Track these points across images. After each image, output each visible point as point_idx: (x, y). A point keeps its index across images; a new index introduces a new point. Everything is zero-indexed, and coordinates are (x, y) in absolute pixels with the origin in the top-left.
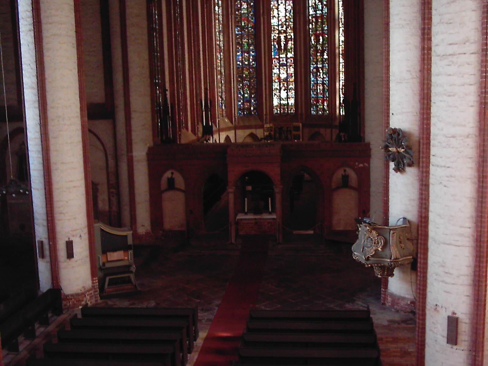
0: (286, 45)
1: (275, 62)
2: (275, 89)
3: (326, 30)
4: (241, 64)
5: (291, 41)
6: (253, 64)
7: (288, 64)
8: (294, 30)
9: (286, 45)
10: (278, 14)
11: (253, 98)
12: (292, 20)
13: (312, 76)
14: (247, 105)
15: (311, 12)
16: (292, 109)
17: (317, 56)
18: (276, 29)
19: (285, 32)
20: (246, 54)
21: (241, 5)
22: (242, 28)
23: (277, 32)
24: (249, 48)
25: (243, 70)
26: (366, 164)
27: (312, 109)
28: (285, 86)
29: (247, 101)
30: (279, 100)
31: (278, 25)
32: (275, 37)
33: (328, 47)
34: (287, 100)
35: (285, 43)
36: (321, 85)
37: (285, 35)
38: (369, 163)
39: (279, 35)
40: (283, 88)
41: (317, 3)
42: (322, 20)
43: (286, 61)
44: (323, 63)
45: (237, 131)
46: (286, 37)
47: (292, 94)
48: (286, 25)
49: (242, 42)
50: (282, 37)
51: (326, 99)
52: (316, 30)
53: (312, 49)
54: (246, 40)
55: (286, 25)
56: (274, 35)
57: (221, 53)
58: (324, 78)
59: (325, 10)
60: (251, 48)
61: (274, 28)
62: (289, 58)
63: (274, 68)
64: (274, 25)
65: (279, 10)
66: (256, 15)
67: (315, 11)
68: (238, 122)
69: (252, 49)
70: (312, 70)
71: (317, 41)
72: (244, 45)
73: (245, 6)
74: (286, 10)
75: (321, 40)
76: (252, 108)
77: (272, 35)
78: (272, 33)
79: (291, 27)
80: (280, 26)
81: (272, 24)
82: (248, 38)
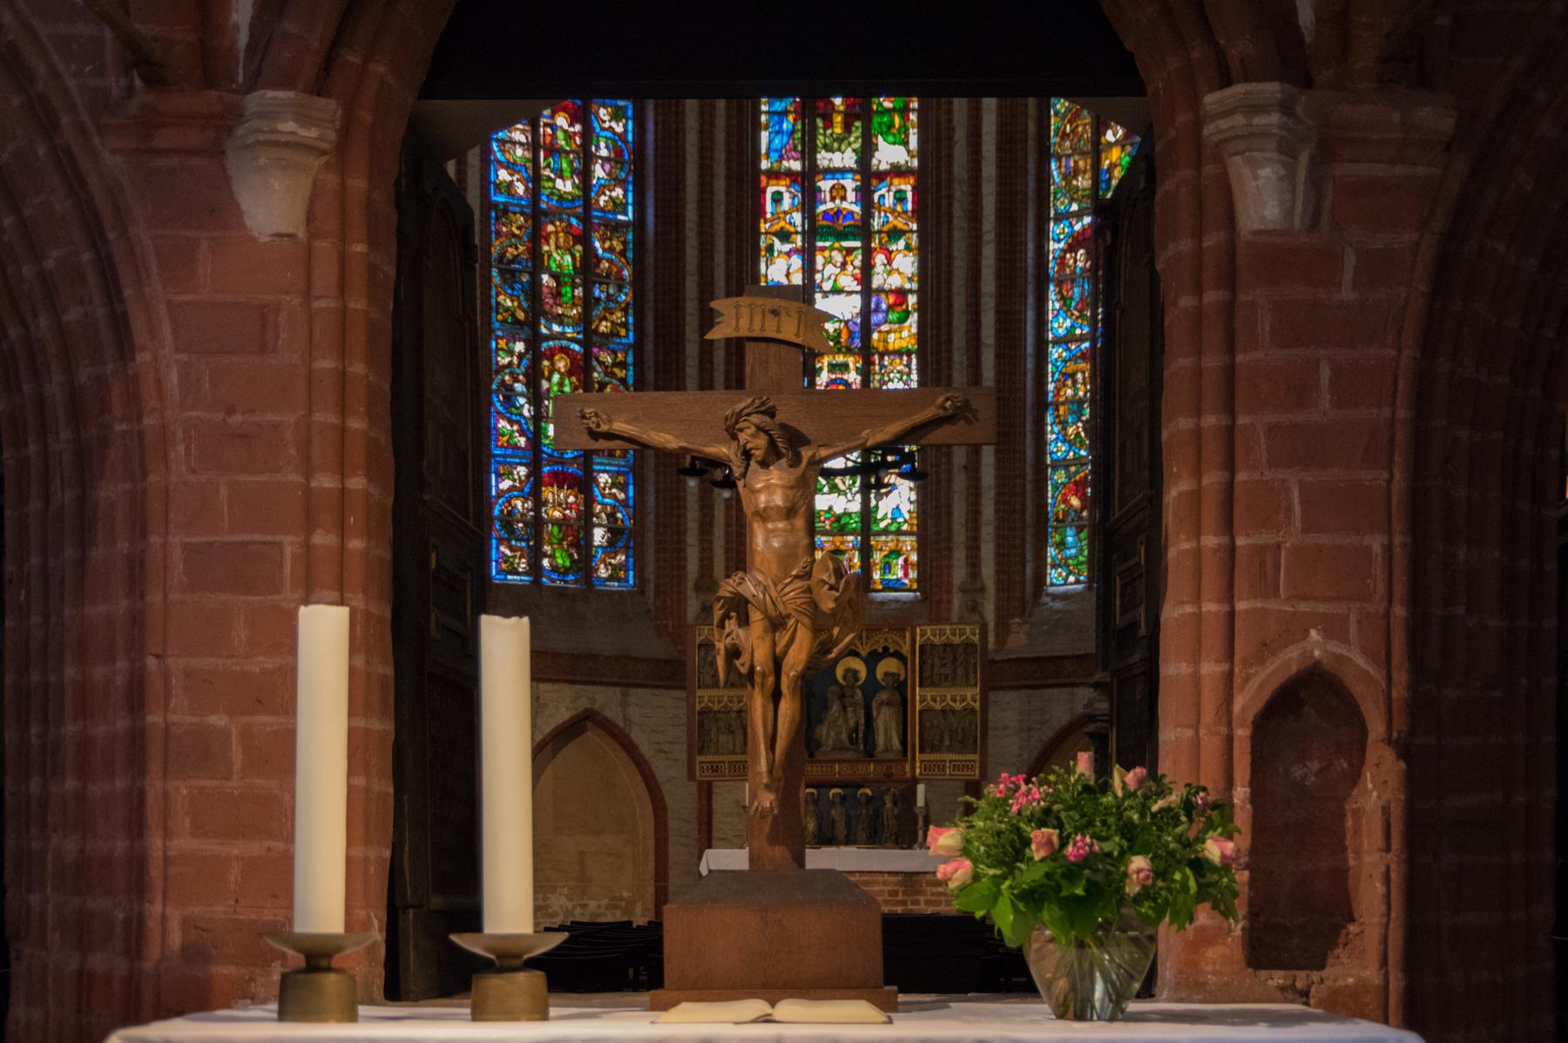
1: (781, 204)
4: (520, 189)
6: (619, 206)
7: (876, 223)
13: (1053, 303)
16: (897, 553)
20: (561, 121)
27: (1051, 551)
29: (560, 480)
43: (865, 194)
62: (881, 176)
63: (770, 248)
70: (1062, 261)
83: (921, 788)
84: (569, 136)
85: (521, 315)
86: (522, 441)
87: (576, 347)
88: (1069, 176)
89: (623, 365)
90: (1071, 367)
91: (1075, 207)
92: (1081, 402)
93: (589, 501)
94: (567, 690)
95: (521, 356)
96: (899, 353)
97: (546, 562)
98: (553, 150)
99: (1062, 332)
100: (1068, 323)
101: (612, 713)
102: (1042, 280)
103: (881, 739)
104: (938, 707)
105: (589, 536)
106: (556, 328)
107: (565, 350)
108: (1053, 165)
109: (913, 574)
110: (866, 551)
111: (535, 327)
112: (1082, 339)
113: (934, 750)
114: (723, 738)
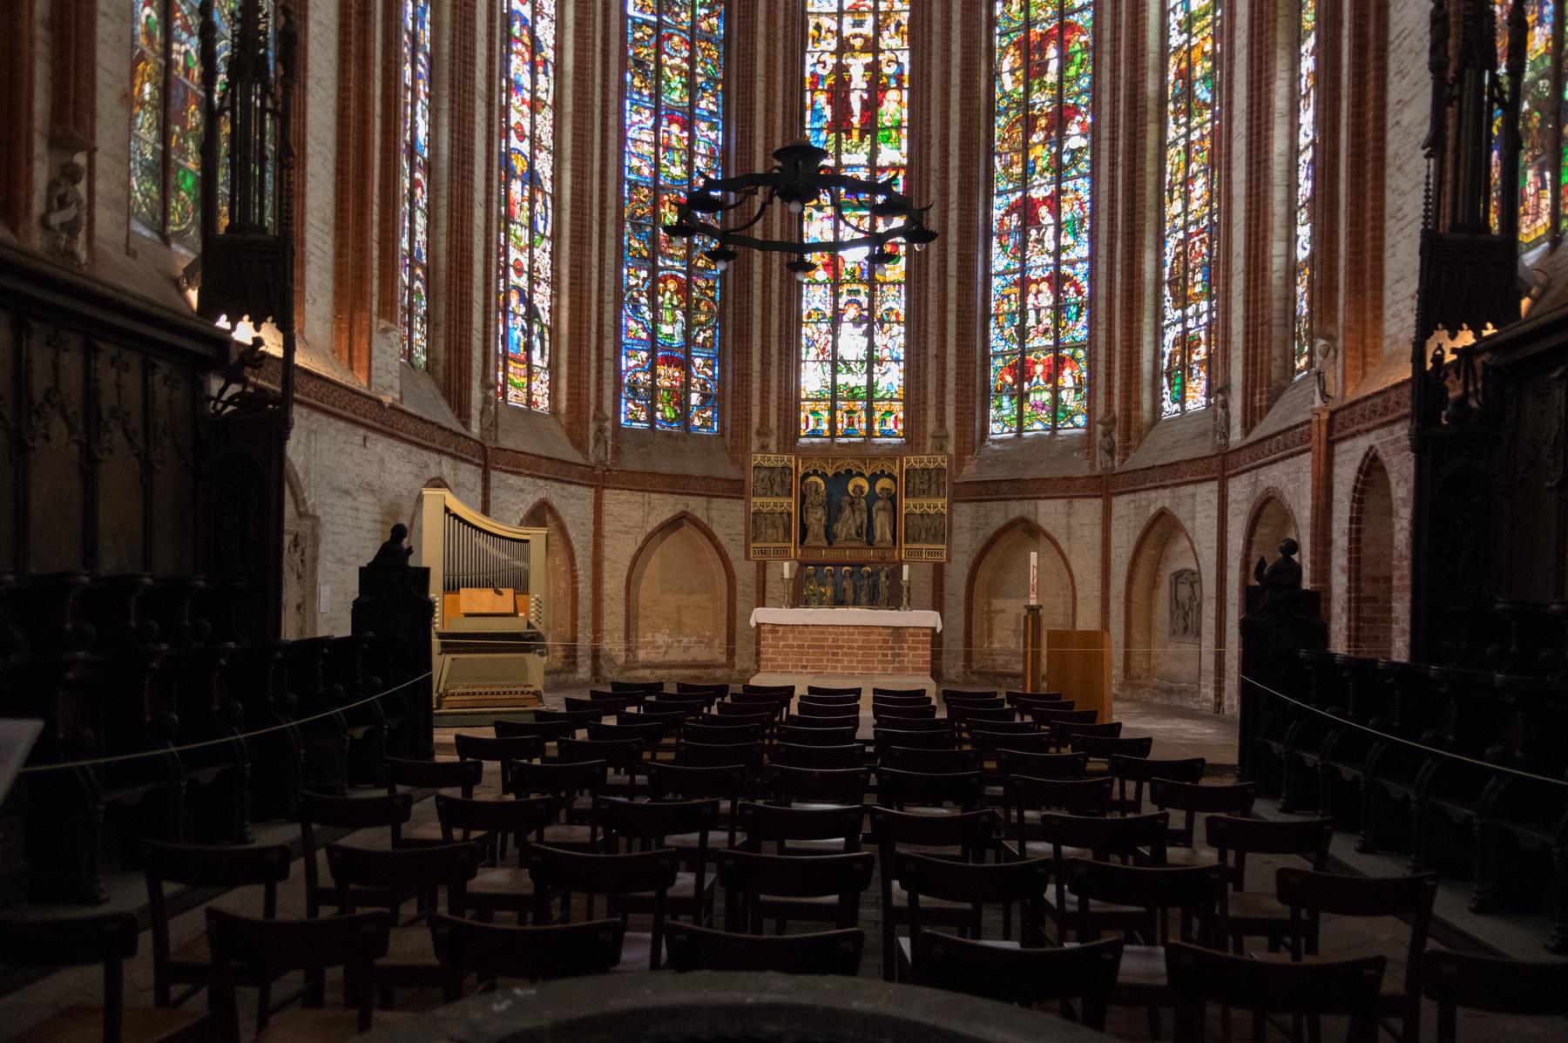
0: (872, 106)
2: (809, 316)
4: (646, 171)
5: (900, 87)
8: (918, 35)
9: (872, 106)
11: (703, 345)
14: (668, 376)
16: (890, 412)
17: (1026, 147)
18: (829, 31)
19: (872, 46)
20: (675, 128)
23: (833, 45)
24: (693, 105)
25: (656, 204)
27: (993, 412)
28: (859, 304)
29: (669, 361)
30: (828, 367)
31: (840, 13)
32: (819, 70)
33: (1094, 89)
34: (870, 372)
35: (865, 96)
36: (1044, 286)
37: (869, 58)
39: (840, 58)
40: (852, 312)
44: (1059, 171)
45: (609, 496)
46: (873, 68)
47: (893, 340)
49: (659, 65)
50: (857, 67)
51: (1073, 357)
52: (1028, 24)
53: (1001, 121)
56: (818, 59)
57: (541, 78)
58: (1059, 249)
60: (703, 104)
61: (818, 27)
63: (810, 216)
64: (819, 14)
68: (617, 451)
69: (711, 112)
71: (1032, 70)
72: (669, 81)
75: (1053, 66)
76: (695, 399)
77: (809, 60)
78: (810, 48)
79: (899, 25)
80: (848, 20)
81: (809, 9)
83: (906, 568)
84: (680, 140)
85: (645, 253)
86: (644, 336)
87: (682, 276)
88: (1008, 166)
89: (713, 288)
90: (1007, 291)
91: (1011, 186)
92: (1013, 314)
93: (689, 375)
94: (670, 499)
95: (644, 280)
96: (893, 283)
97: (658, 415)
98: (668, 148)
99: (1001, 268)
100: (1006, 262)
101: (700, 513)
102: (988, 234)
103: (878, 533)
104: (918, 511)
105: (688, 399)
106: (669, 263)
107: (675, 277)
108: (997, 159)
109: (900, 426)
110: (870, 411)
111: (654, 261)
112: (1014, 272)
113: (915, 541)
114: (770, 532)
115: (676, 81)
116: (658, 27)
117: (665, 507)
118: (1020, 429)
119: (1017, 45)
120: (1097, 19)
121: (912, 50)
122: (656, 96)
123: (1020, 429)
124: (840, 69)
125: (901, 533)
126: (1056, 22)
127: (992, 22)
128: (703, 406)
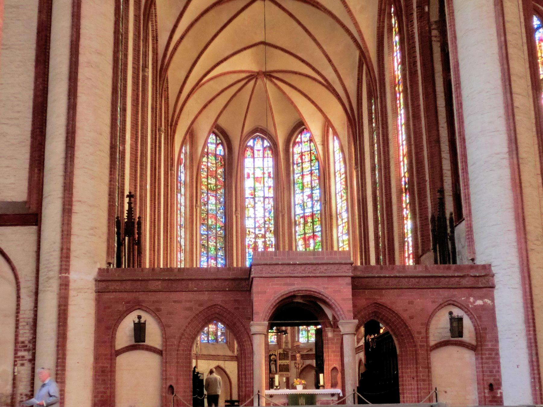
3: (318, 232)
8: (276, 233)
10: (255, 214)
12: (272, 222)
15: (299, 211)
19: (264, 236)
20: (213, 261)
21: (208, 199)
22: (209, 228)
23: (253, 236)
24: (216, 255)
26: (488, 301)
31: (255, 228)
32: (250, 243)
37: (263, 240)
38: (493, 300)
41: (305, 201)
42: (313, 219)
46: (265, 242)
48: (264, 227)
50: (260, 242)
52: (305, 234)
54: (213, 243)
55: (264, 227)
59: (317, 207)
60: (219, 254)
61: (249, 231)
65: (256, 209)
66: (227, 214)
67: (304, 210)
68: (201, 349)
69: (222, 256)
73: (212, 200)
74: (265, 210)
77: (247, 240)
80: (257, 229)
82: (216, 240)
84: (214, 264)
113: (282, 371)
115: (213, 248)
116: (207, 235)
117: (213, 364)
118: (308, 340)
119: (303, 238)
120: (322, 234)
121: (275, 237)
122: (207, 253)
123: (308, 340)
124: (255, 243)
125: (278, 369)
126: (312, 234)
127: (296, 232)
128: (222, 335)
